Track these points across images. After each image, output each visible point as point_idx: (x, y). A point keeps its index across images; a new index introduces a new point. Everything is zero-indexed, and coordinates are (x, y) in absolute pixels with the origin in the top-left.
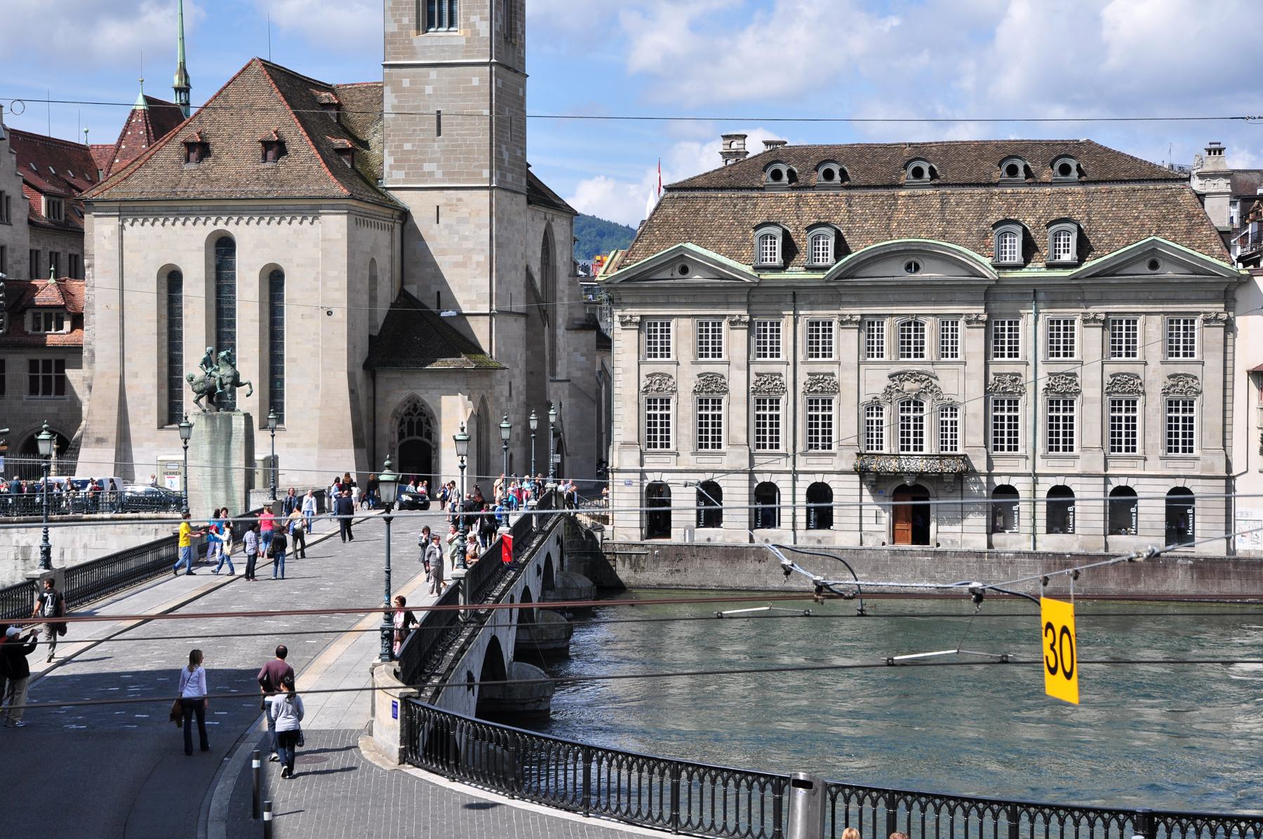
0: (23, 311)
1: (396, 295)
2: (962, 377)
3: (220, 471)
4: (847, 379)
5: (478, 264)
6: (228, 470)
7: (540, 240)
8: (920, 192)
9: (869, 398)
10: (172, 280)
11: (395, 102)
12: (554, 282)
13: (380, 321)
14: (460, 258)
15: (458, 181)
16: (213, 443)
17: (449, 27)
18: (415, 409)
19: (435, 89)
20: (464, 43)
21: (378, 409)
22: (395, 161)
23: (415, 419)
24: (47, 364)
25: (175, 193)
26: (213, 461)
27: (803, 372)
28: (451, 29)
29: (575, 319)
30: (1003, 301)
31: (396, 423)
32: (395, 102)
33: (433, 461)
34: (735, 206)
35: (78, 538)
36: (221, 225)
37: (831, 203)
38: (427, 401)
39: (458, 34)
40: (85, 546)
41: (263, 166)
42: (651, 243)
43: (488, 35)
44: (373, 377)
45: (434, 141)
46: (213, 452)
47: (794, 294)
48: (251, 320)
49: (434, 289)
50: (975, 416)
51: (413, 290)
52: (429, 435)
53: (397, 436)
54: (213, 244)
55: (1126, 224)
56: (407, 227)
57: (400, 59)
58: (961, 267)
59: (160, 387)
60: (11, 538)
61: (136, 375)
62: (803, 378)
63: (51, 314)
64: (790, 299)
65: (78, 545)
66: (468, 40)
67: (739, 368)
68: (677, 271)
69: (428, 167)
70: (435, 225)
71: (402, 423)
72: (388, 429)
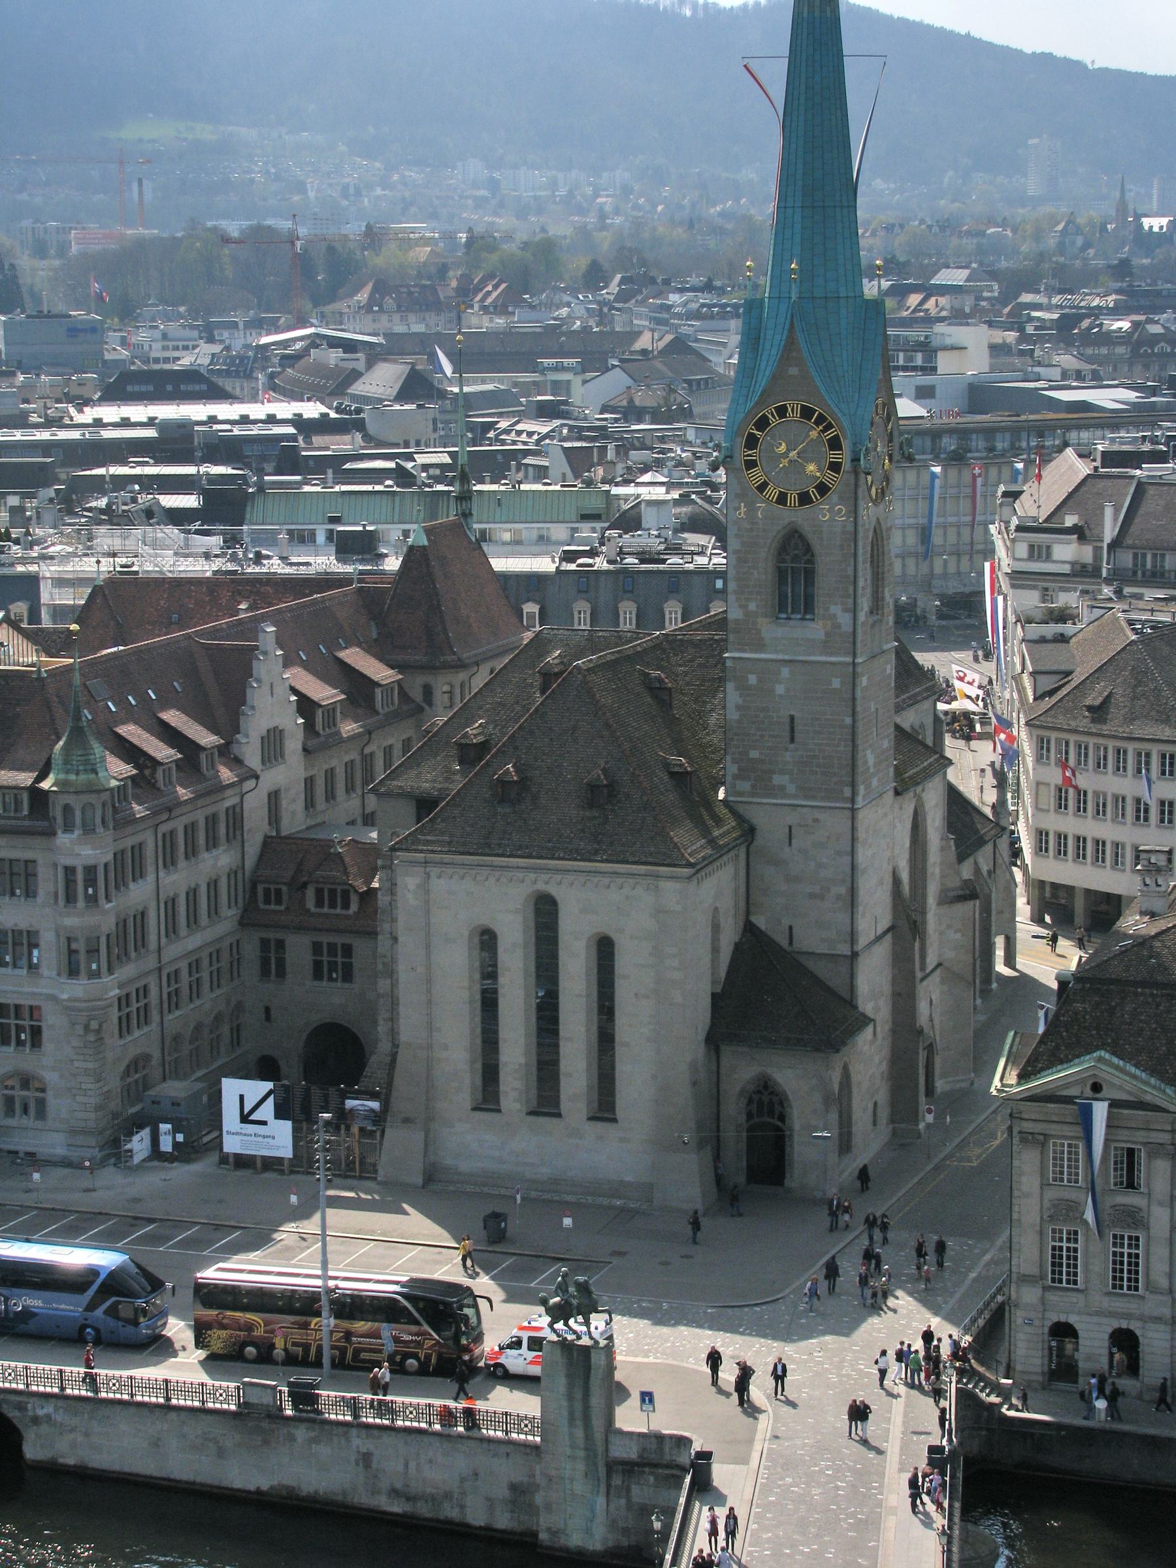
0: (304, 886)
1: (740, 929)
3: (578, 1406)
5: (839, 897)
6: (586, 1408)
7: (908, 825)
10: (487, 940)
11: (740, 701)
12: (925, 854)
13: (723, 975)
14: (817, 889)
15: (814, 798)
16: (569, 1376)
17: (806, 612)
18: (766, 1087)
19: (787, 690)
20: (823, 637)
21: (723, 1086)
22: (739, 770)
23: (766, 1098)
24: (332, 948)
25: (489, 845)
26: (570, 1397)
28: (808, 617)
29: (948, 890)
31: (744, 1101)
32: (740, 701)
33: (788, 1150)
34: (1158, 1006)
36: (541, 886)
38: (779, 1080)
39: (816, 630)
41: (588, 814)
42: (1057, 1048)
43: (851, 630)
44: (717, 1051)
45: (787, 750)
46: (571, 1386)
48: (577, 996)
49: (786, 922)
51: (760, 921)
52: (782, 1118)
53: (744, 1117)
54: (532, 903)
56: (752, 848)
57: (744, 651)
59: (473, 1062)
61: (446, 1047)
63: (335, 890)
66: (827, 634)
67: (1160, 1204)
69: (777, 780)
70: (787, 849)
71: (750, 1101)
72: (734, 1110)
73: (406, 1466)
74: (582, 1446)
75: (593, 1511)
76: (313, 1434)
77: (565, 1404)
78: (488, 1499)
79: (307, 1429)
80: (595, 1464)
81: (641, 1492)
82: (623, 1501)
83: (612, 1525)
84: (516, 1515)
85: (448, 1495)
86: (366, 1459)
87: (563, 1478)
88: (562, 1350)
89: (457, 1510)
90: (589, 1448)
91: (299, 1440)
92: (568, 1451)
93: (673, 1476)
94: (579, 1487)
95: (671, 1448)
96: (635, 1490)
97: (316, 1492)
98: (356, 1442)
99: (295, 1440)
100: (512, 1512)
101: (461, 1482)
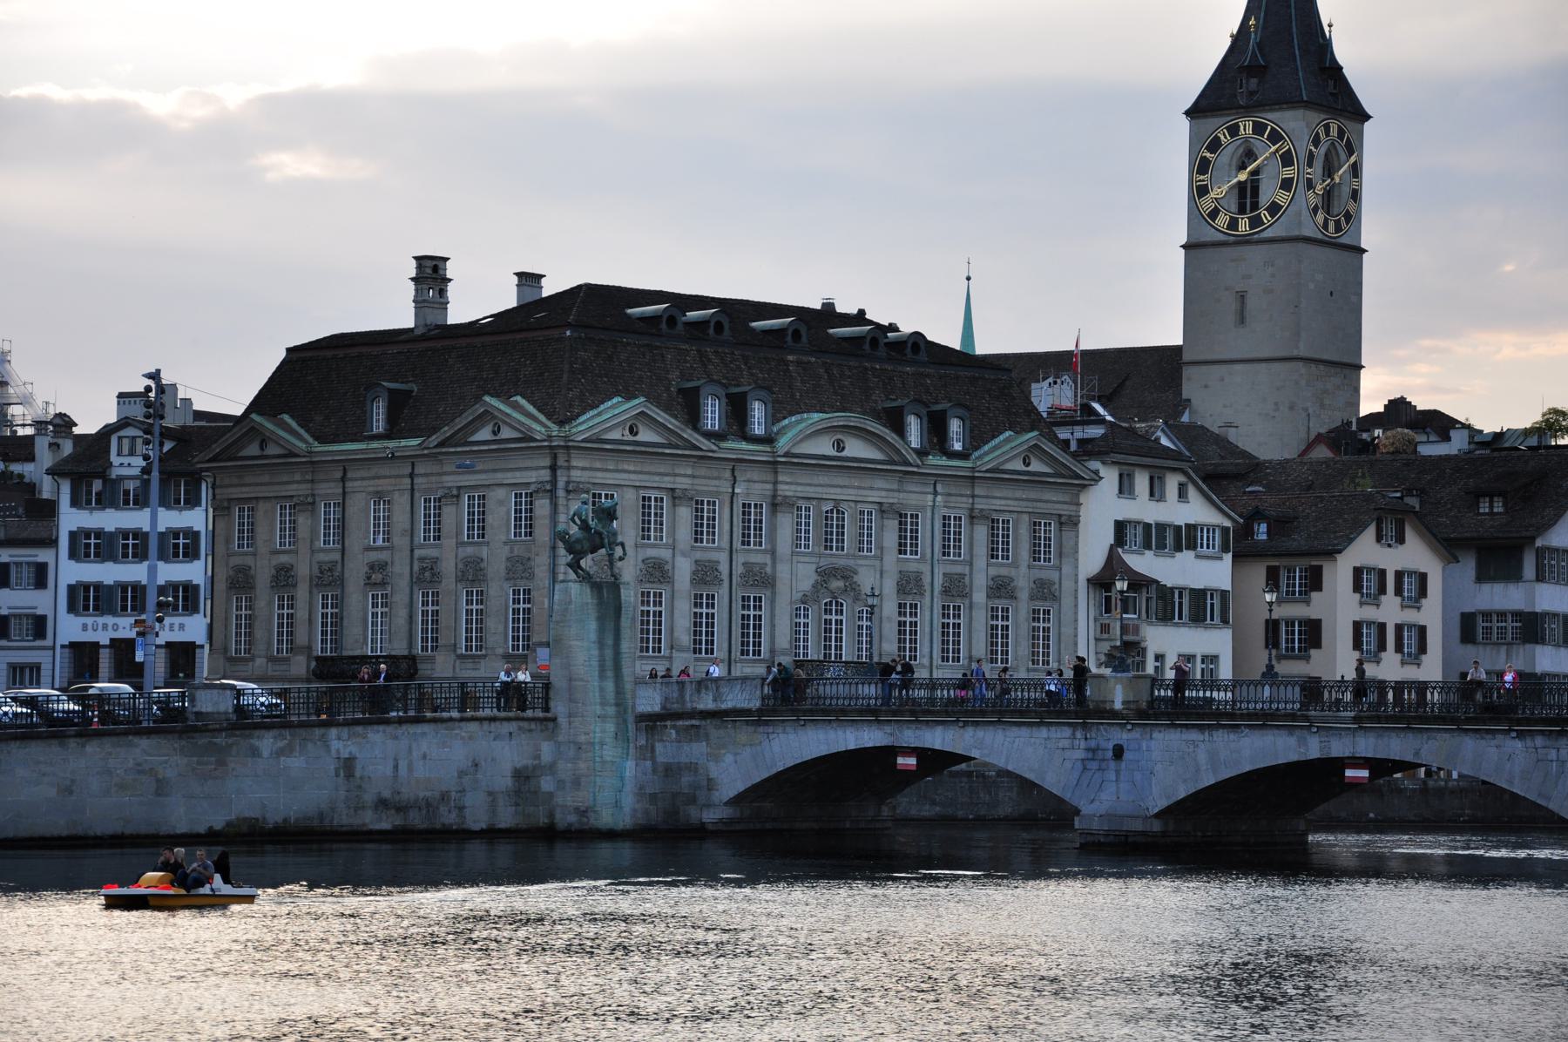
2: (878, 576)
3: (609, 653)
4: (783, 571)
8: (805, 359)
9: (800, 595)
16: (601, 619)
26: (601, 644)
27: (740, 559)
30: (911, 492)
35: (414, 746)
37: (731, 362)
40: (424, 757)
46: (601, 630)
47: (733, 470)
50: (889, 619)
55: (983, 415)
58: (880, 449)
60: (328, 747)
62: (739, 570)
64: (728, 474)
65: (414, 754)
67: (684, 554)
68: (627, 432)
73: (396, 767)
74: (613, 701)
75: (622, 778)
76: (281, 744)
77: (595, 652)
78: (490, 794)
79: (275, 738)
80: (625, 721)
81: (667, 749)
82: (649, 763)
83: (640, 792)
84: (520, 808)
85: (444, 797)
86: (348, 765)
87: (593, 744)
88: (592, 588)
89: (453, 815)
90: (620, 703)
91: (266, 754)
92: (598, 710)
93: (693, 726)
94: (609, 753)
95: (691, 695)
96: (659, 747)
97: (285, 820)
98: (335, 745)
99: (260, 756)
100: (517, 805)
101: (459, 777)
